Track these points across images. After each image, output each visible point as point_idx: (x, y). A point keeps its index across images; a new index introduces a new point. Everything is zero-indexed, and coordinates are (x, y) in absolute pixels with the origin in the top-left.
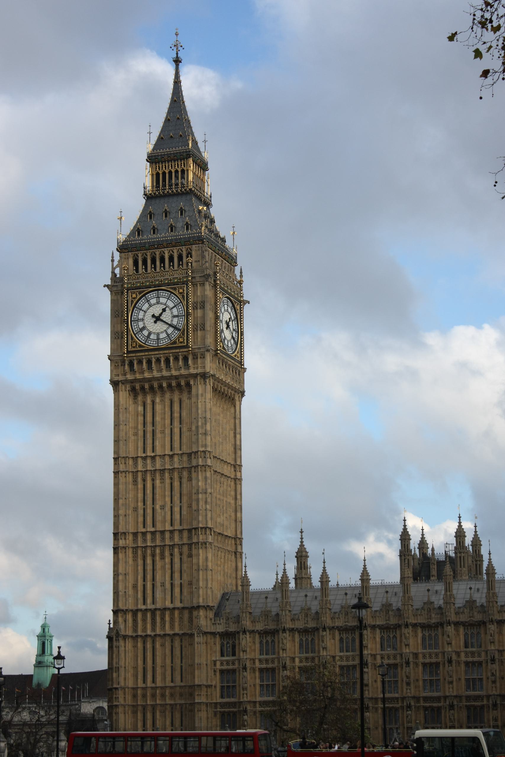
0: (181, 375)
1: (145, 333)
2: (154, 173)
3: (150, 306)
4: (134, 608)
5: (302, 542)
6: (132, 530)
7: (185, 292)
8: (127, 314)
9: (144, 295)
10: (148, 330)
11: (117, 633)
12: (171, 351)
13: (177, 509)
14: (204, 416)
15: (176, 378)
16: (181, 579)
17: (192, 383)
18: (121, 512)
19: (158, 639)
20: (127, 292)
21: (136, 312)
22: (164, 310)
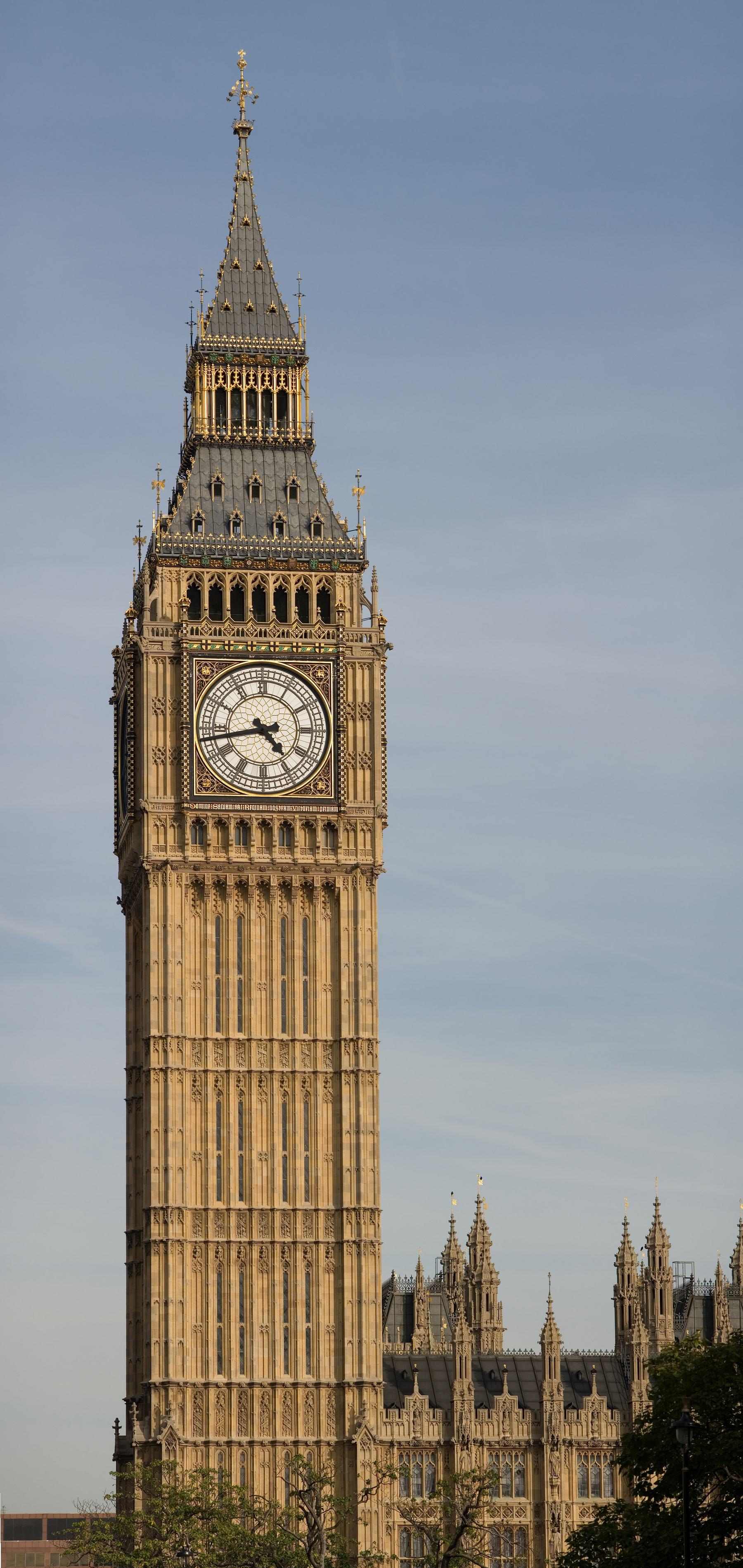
1: (233, 759)
2: (214, 388)
3: (244, 698)
6: (193, 1202)
11: (172, 1434)
13: (300, 1164)
14: (369, 960)
15: (305, 869)
17: (339, 884)
18: (171, 1160)
20: (190, 660)
21: (210, 708)
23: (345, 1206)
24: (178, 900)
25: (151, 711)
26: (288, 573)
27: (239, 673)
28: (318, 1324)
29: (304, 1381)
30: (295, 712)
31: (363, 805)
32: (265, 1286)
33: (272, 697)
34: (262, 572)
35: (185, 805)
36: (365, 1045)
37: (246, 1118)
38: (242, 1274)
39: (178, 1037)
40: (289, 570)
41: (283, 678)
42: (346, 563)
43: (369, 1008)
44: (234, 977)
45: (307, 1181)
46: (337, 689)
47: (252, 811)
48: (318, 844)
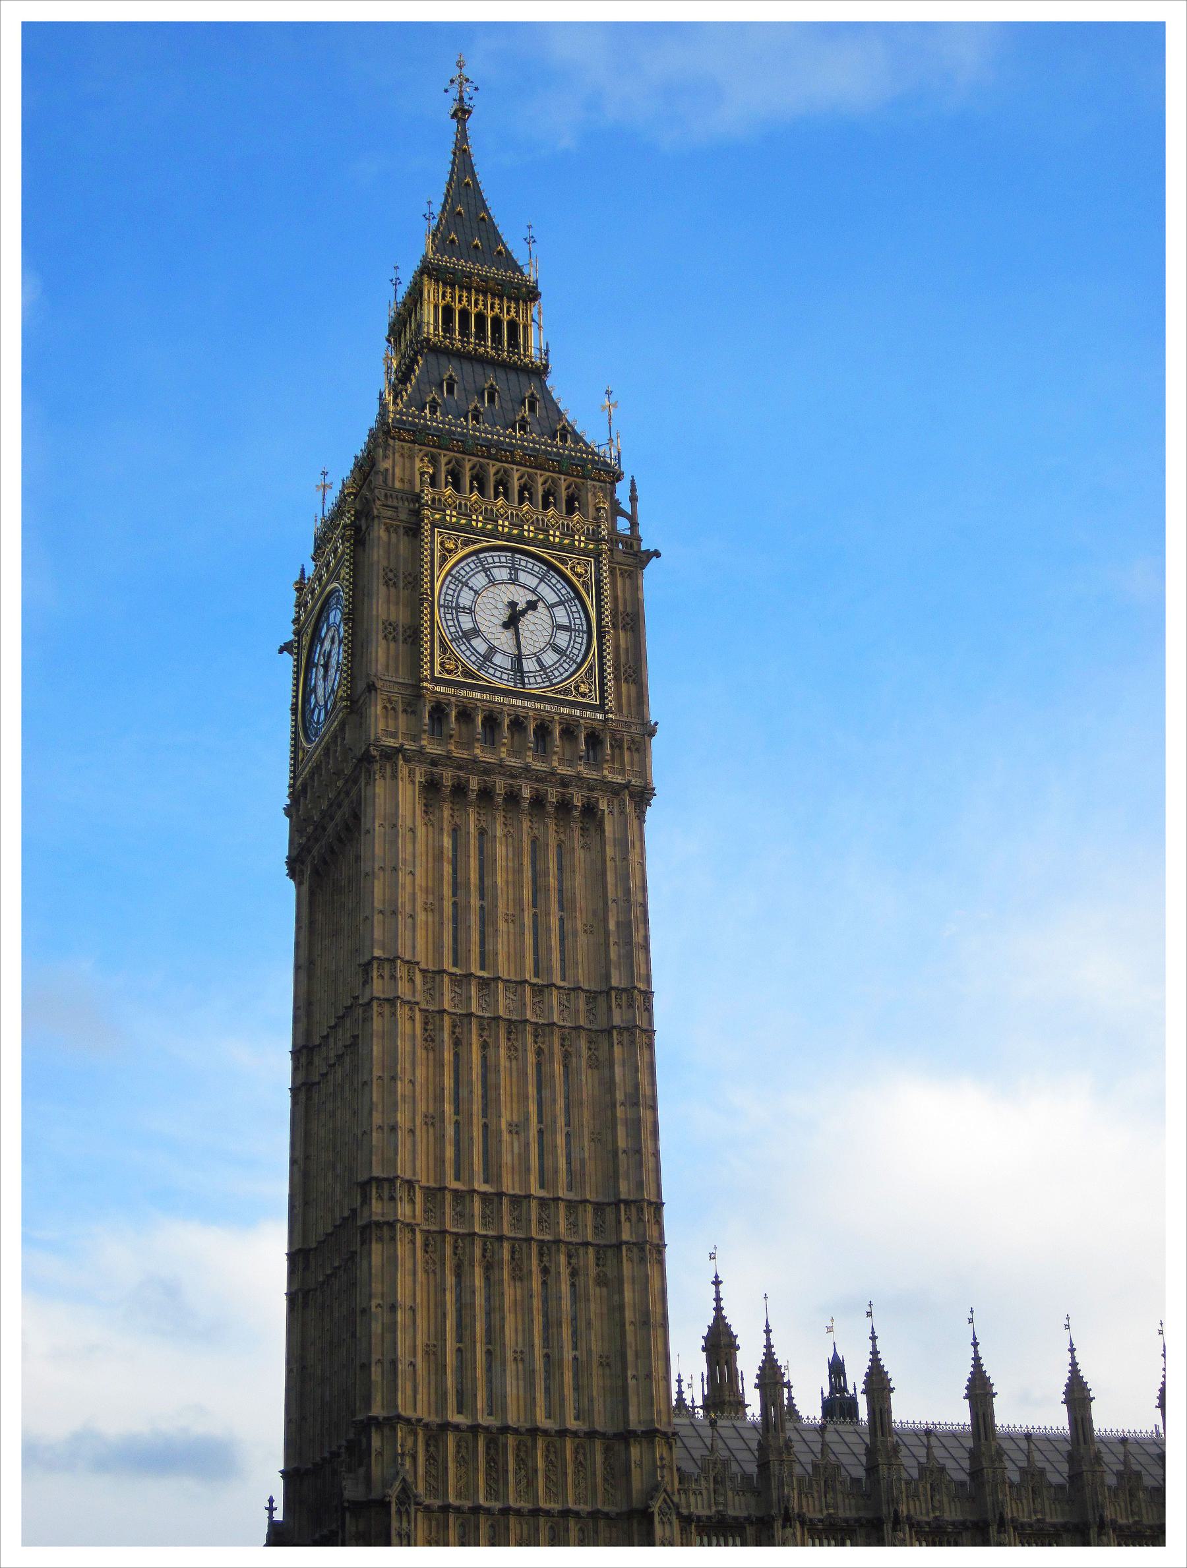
0: (579, 777)
1: (480, 646)
3: (492, 582)
4: (434, 1419)
5: (718, 1309)
6: (424, 1179)
10: (486, 640)
11: (405, 1490)
13: (561, 1140)
14: (640, 899)
15: (564, 782)
16: (575, 1348)
17: (603, 805)
19: (512, 1521)
22: (532, 606)
23: (623, 1197)
24: (409, 799)
25: (381, 581)
27: (486, 554)
28: (589, 1351)
29: (574, 1428)
30: (550, 607)
32: (519, 1298)
33: (523, 586)
34: (506, 465)
35: (425, 684)
37: (491, 1077)
38: (487, 1279)
41: (536, 569)
42: (600, 470)
43: (642, 956)
45: (569, 1162)
46: (599, 588)
47: (504, 704)
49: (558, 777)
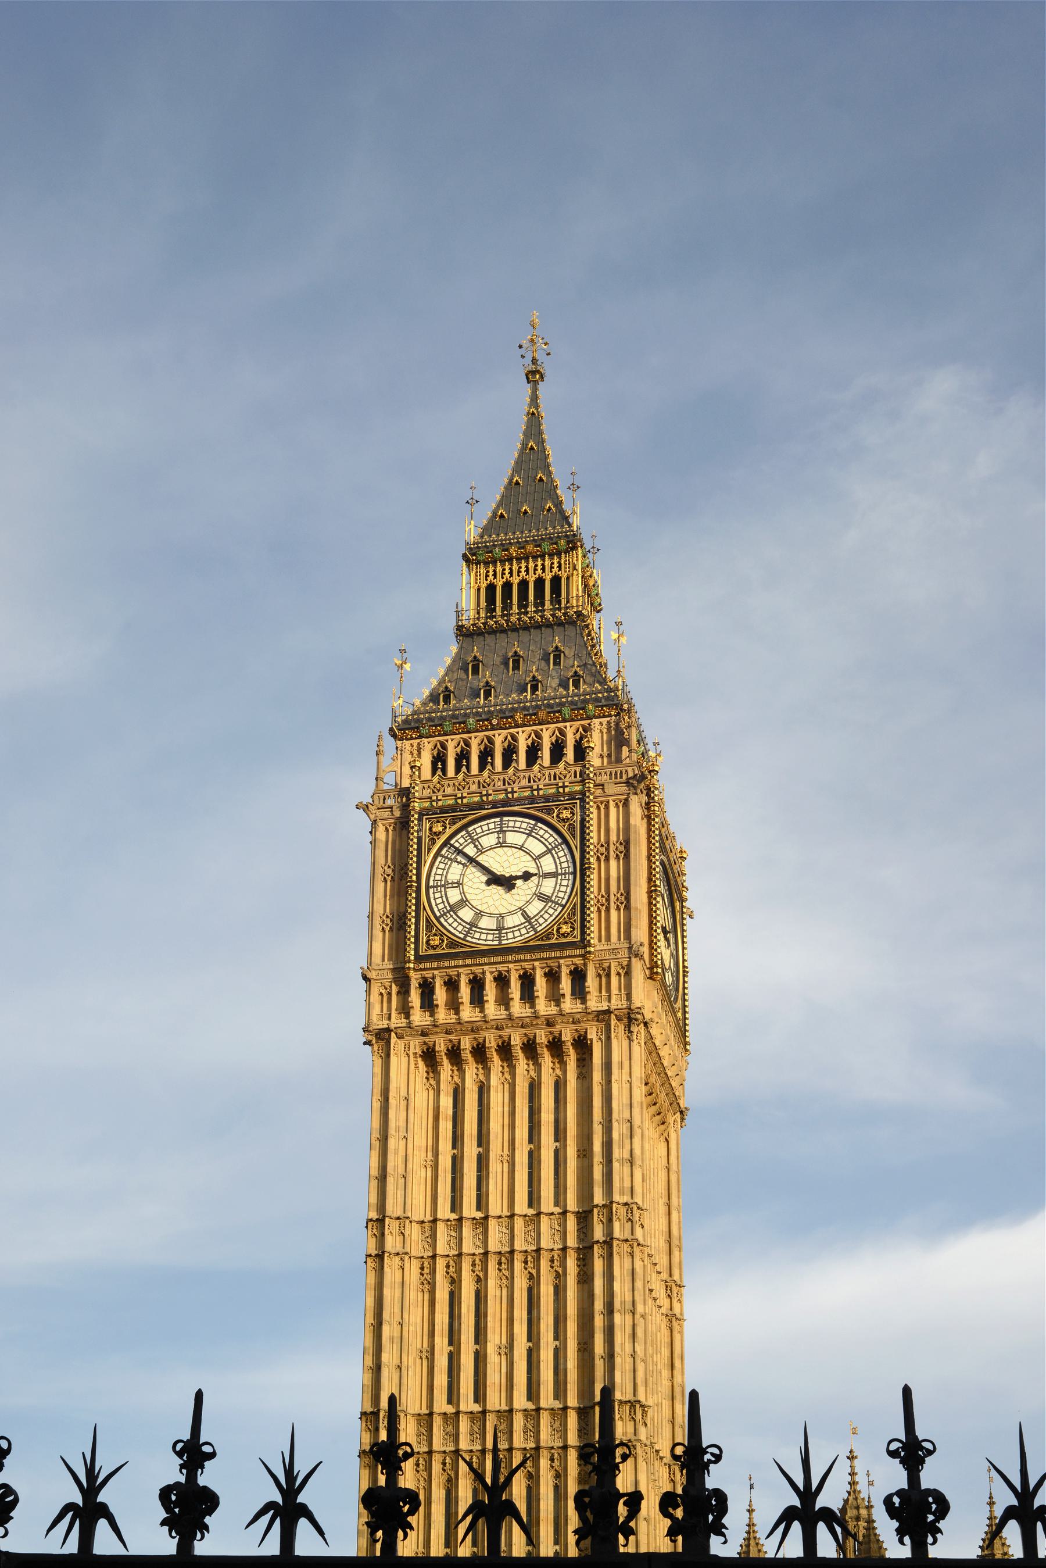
7: (578, 818)
8: (419, 869)
9: (465, 827)
12: (538, 956)
13: (546, 1356)
15: (549, 1023)
17: (592, 1034)
18: (385, 1357)
20: (420, 819)
21: (442, 866)
24: (404, 1071)
26: (540, 727)
27: (476, 826)
31: (618, 946)
34: (511, 731)
36: (622, 1210)
39: (398, 1218)
40: (540, 724)
44: (471, 1150)
48: (562, 992)
49: (543, 1019)
